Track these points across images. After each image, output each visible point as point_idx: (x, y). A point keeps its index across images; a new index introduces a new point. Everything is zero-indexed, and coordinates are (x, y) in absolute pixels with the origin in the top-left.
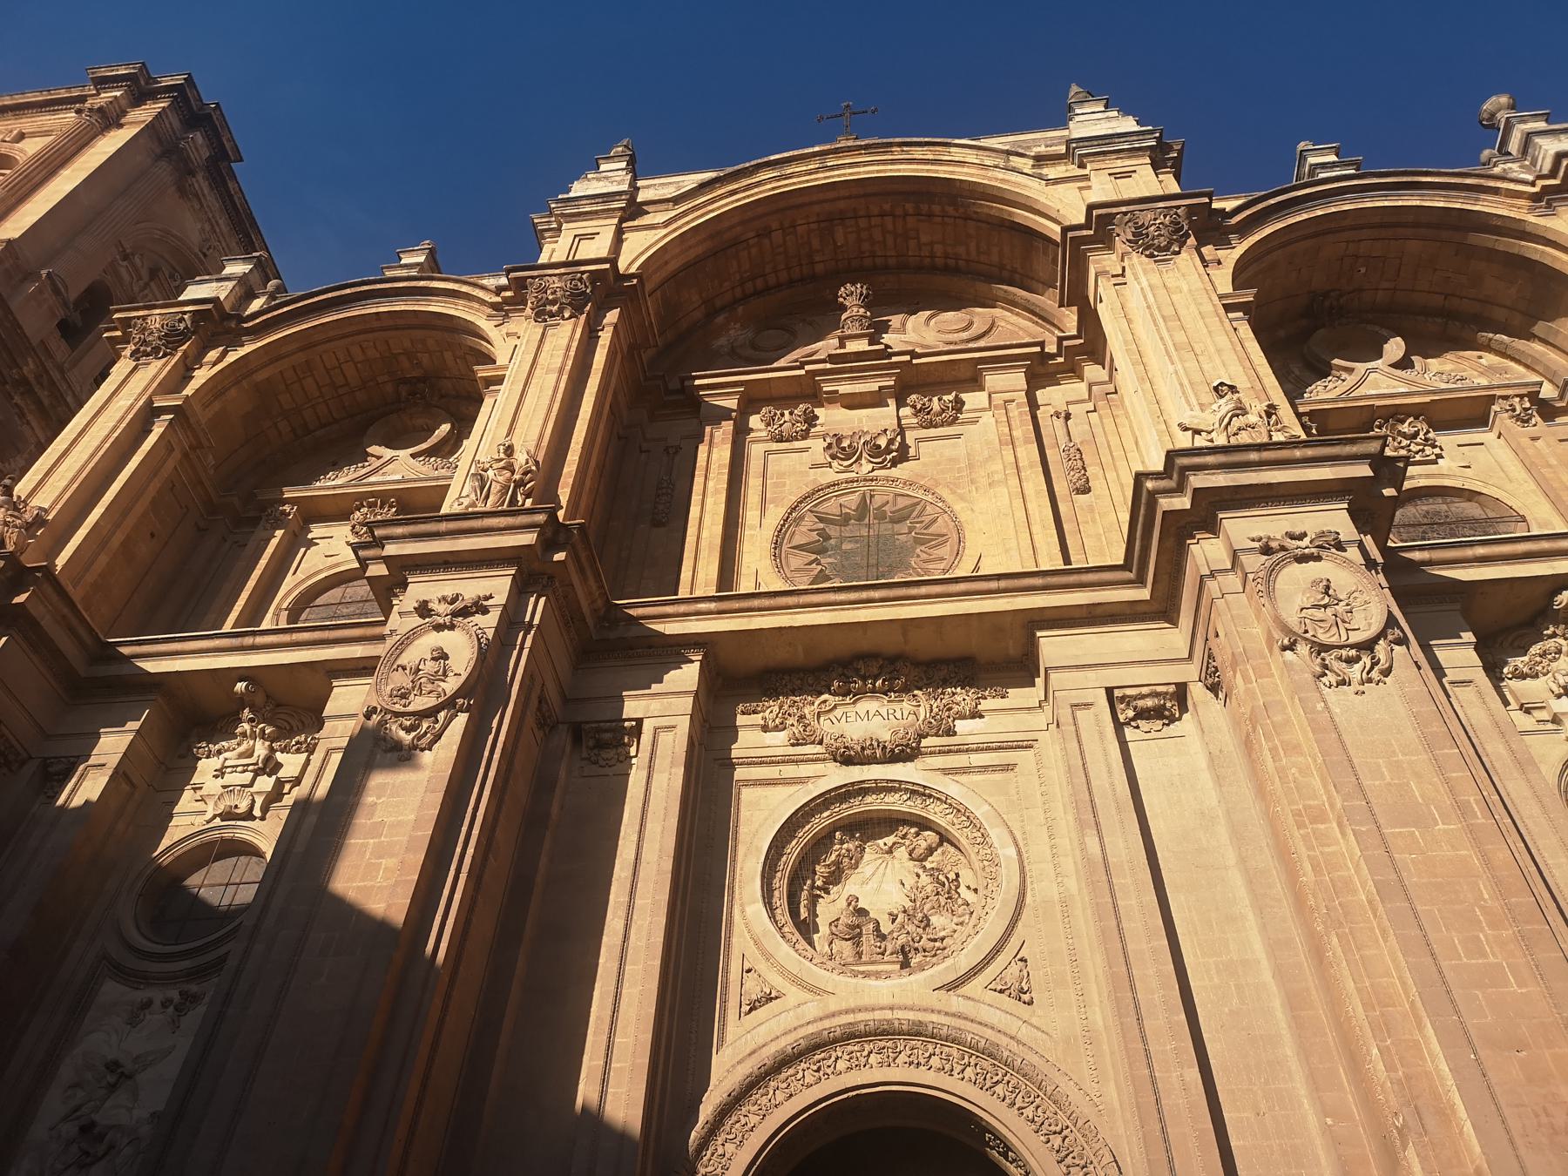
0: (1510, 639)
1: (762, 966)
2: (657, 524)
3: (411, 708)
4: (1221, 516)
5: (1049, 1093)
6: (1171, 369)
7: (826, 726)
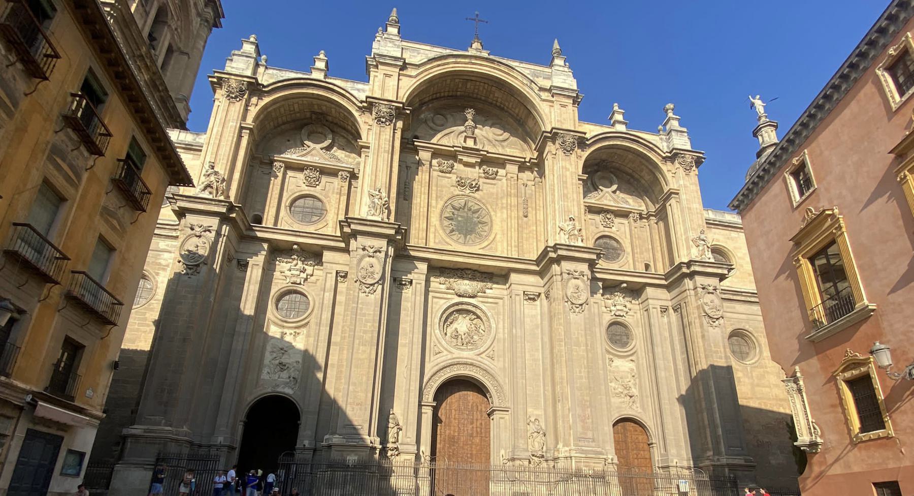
1: (438, 345)
7: (455, 285)
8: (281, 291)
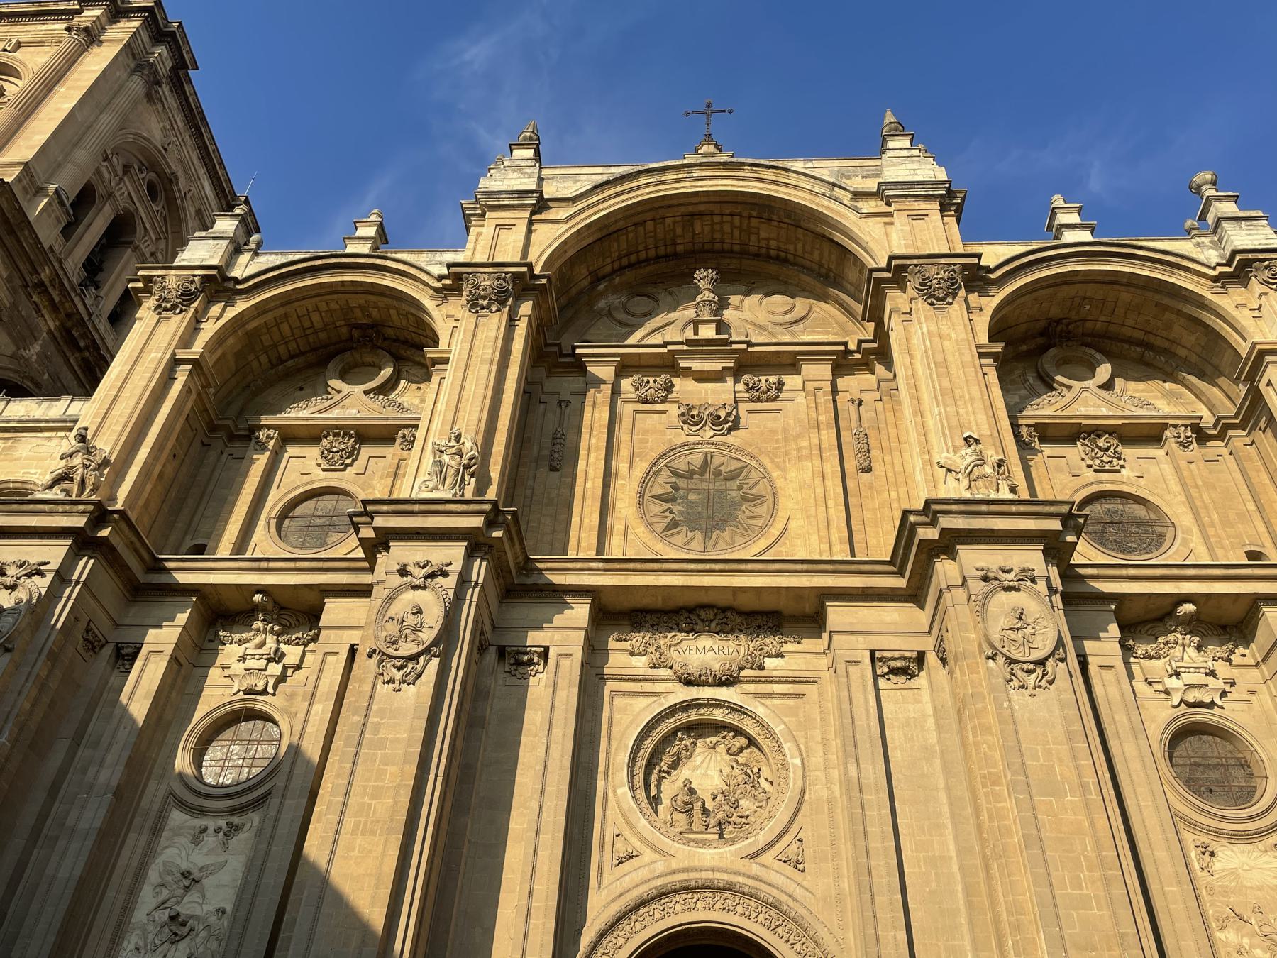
0: (1146, 628)
1: (627, 833)
2: (553, 469)
3: (399, 653)
5: (811, 935)
6: (936, 410)
7: (674, 656)
8: (215, 715)
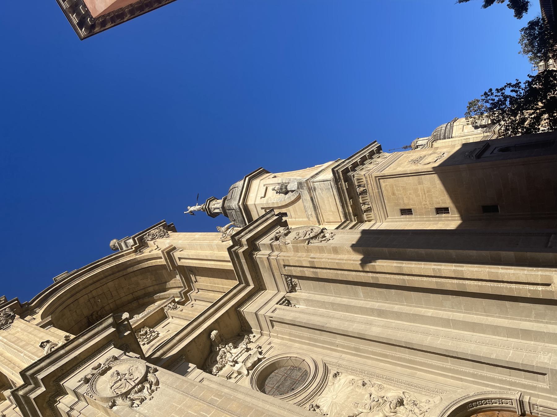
4: (61, 383)
6: (22, 355)
